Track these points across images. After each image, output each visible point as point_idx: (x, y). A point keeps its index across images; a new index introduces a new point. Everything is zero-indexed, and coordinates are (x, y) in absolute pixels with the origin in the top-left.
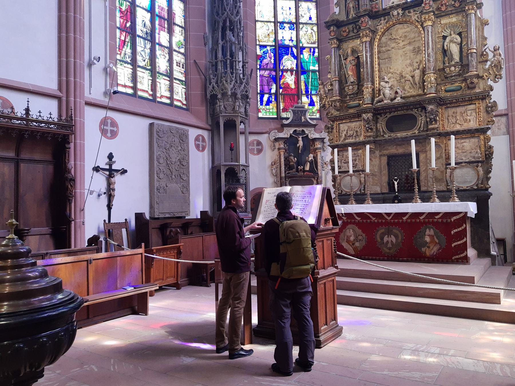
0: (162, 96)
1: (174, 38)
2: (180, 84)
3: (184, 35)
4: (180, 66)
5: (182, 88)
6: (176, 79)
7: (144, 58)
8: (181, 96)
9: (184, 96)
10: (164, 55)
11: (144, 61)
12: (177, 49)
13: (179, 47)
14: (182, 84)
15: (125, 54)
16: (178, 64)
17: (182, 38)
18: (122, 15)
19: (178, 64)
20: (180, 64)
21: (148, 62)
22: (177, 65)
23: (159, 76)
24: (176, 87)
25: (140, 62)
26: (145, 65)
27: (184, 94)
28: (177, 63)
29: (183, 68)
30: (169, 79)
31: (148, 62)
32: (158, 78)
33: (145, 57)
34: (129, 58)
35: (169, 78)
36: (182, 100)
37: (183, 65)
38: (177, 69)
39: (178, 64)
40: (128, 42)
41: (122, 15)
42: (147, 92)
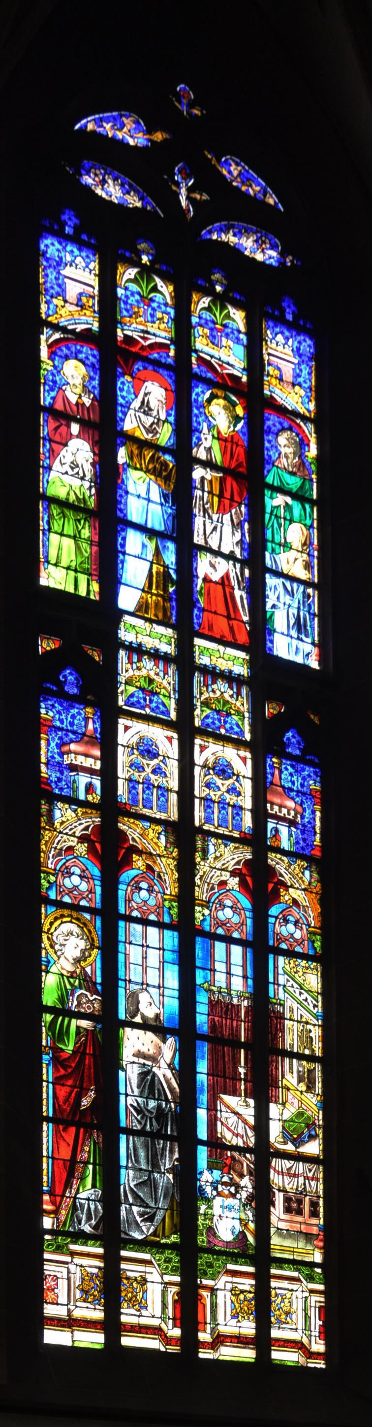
0: (219, 1340)
1: (274, 1110)
2: (298, 1280)
3: (319, 1086)
4: (300, 1212)
5: (307, 1294)
6: (281, 1262)
7: (148, 1210)
8: (301, 1325)
9: (316, 1323)
10: (232, 1183)
11: (151, 1219)
12: (290, 1147)
13: (299, 1136)
14: (311, 1278)
15: (74, 1208)
16: (293, 1206)
17: (312, 1102)
18: (62, 1072)
19: (295, 1205)
20: (300, 1202)
21: (164, 1220)
22: (288, 1210)
23: (210, 1265)
24: (278, 1291)
25: (133, 1226)
26: (155, 1234)
27: (314, 1314)
28: (287, 1200)
29: (314, 1214)
30: (251, 1269)
31: (164, 1220)
32: (205, 1273)
33: (153, 1205)
34: (89, 1218)
35: (251, 1260)
36: (305, 1341)
37: (314, 1205)
38: (282, 1225)
39: (295, 1205)
40: (86, 1163)
41: (62, 1072)
42: (156, 1331)
